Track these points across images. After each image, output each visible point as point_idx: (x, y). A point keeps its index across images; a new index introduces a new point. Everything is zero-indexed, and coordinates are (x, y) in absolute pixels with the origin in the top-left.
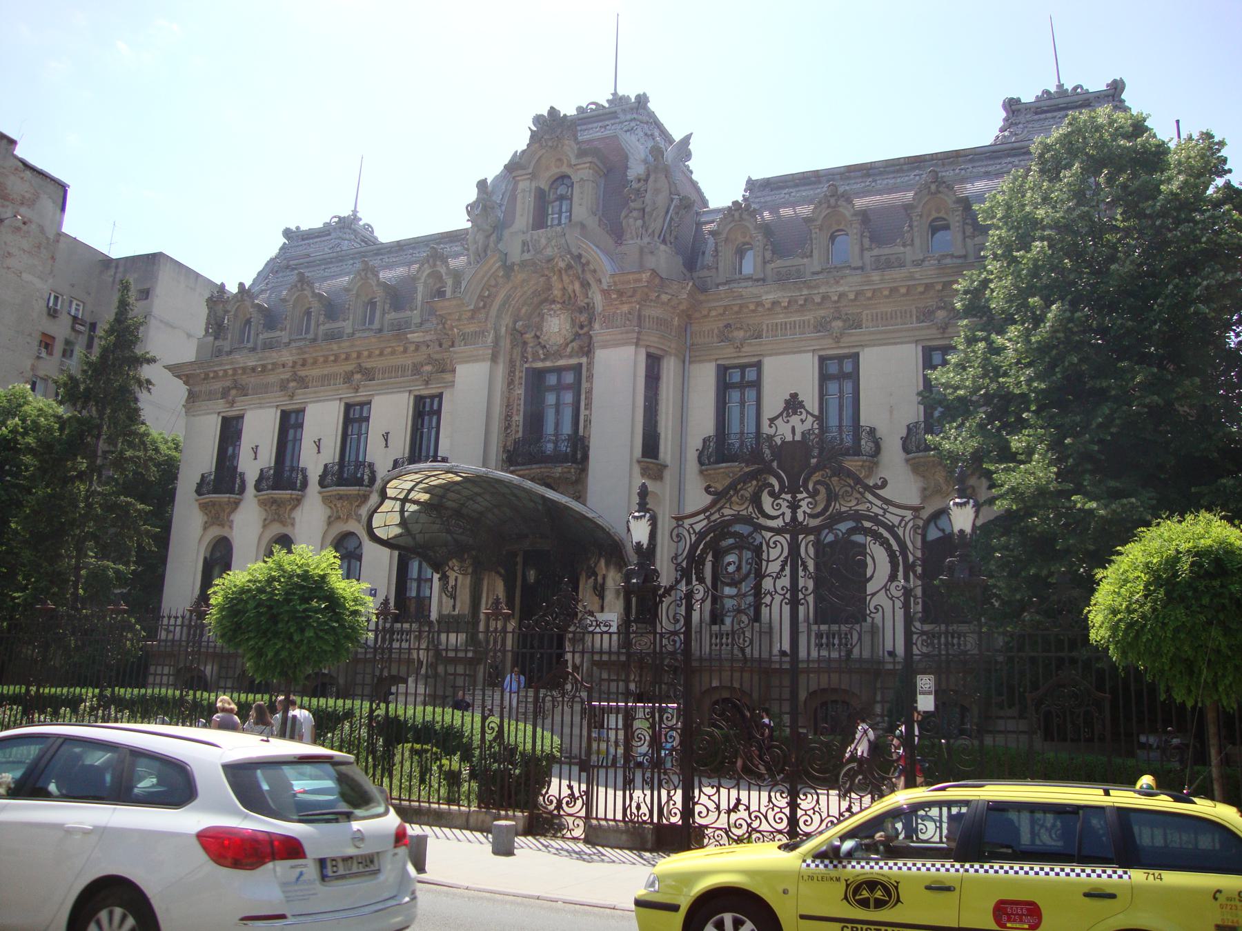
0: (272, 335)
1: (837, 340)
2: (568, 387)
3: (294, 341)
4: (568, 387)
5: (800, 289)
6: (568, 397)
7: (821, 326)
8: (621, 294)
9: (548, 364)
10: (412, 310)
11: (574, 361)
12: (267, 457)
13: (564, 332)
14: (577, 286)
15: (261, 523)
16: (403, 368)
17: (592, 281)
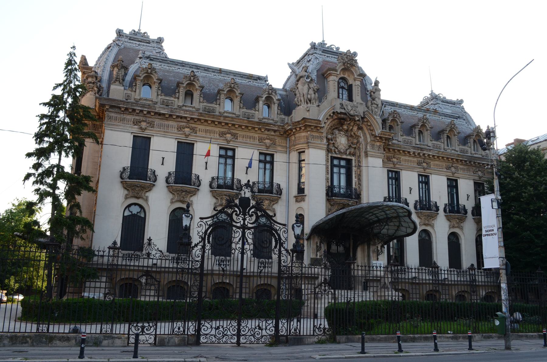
0: (168, 98)
1: (424, 169)
2: (343, 167)
3: (186, 106)
4: (343, 167)
5: (418, 150)
6: (343, 171)
7: (419, 164)
8: (381, 138)
9: (339, 156)
10: (255, 111)
11: (349, 157)
12: (171, 166)
13: (345, 145)
14: (355, 128)
15: (169, 200)
16: (254, 138)
17: (365, 128)
